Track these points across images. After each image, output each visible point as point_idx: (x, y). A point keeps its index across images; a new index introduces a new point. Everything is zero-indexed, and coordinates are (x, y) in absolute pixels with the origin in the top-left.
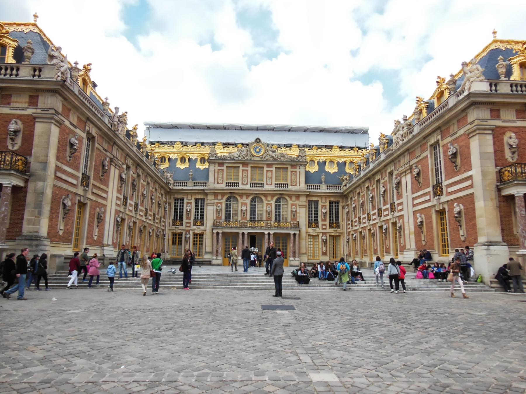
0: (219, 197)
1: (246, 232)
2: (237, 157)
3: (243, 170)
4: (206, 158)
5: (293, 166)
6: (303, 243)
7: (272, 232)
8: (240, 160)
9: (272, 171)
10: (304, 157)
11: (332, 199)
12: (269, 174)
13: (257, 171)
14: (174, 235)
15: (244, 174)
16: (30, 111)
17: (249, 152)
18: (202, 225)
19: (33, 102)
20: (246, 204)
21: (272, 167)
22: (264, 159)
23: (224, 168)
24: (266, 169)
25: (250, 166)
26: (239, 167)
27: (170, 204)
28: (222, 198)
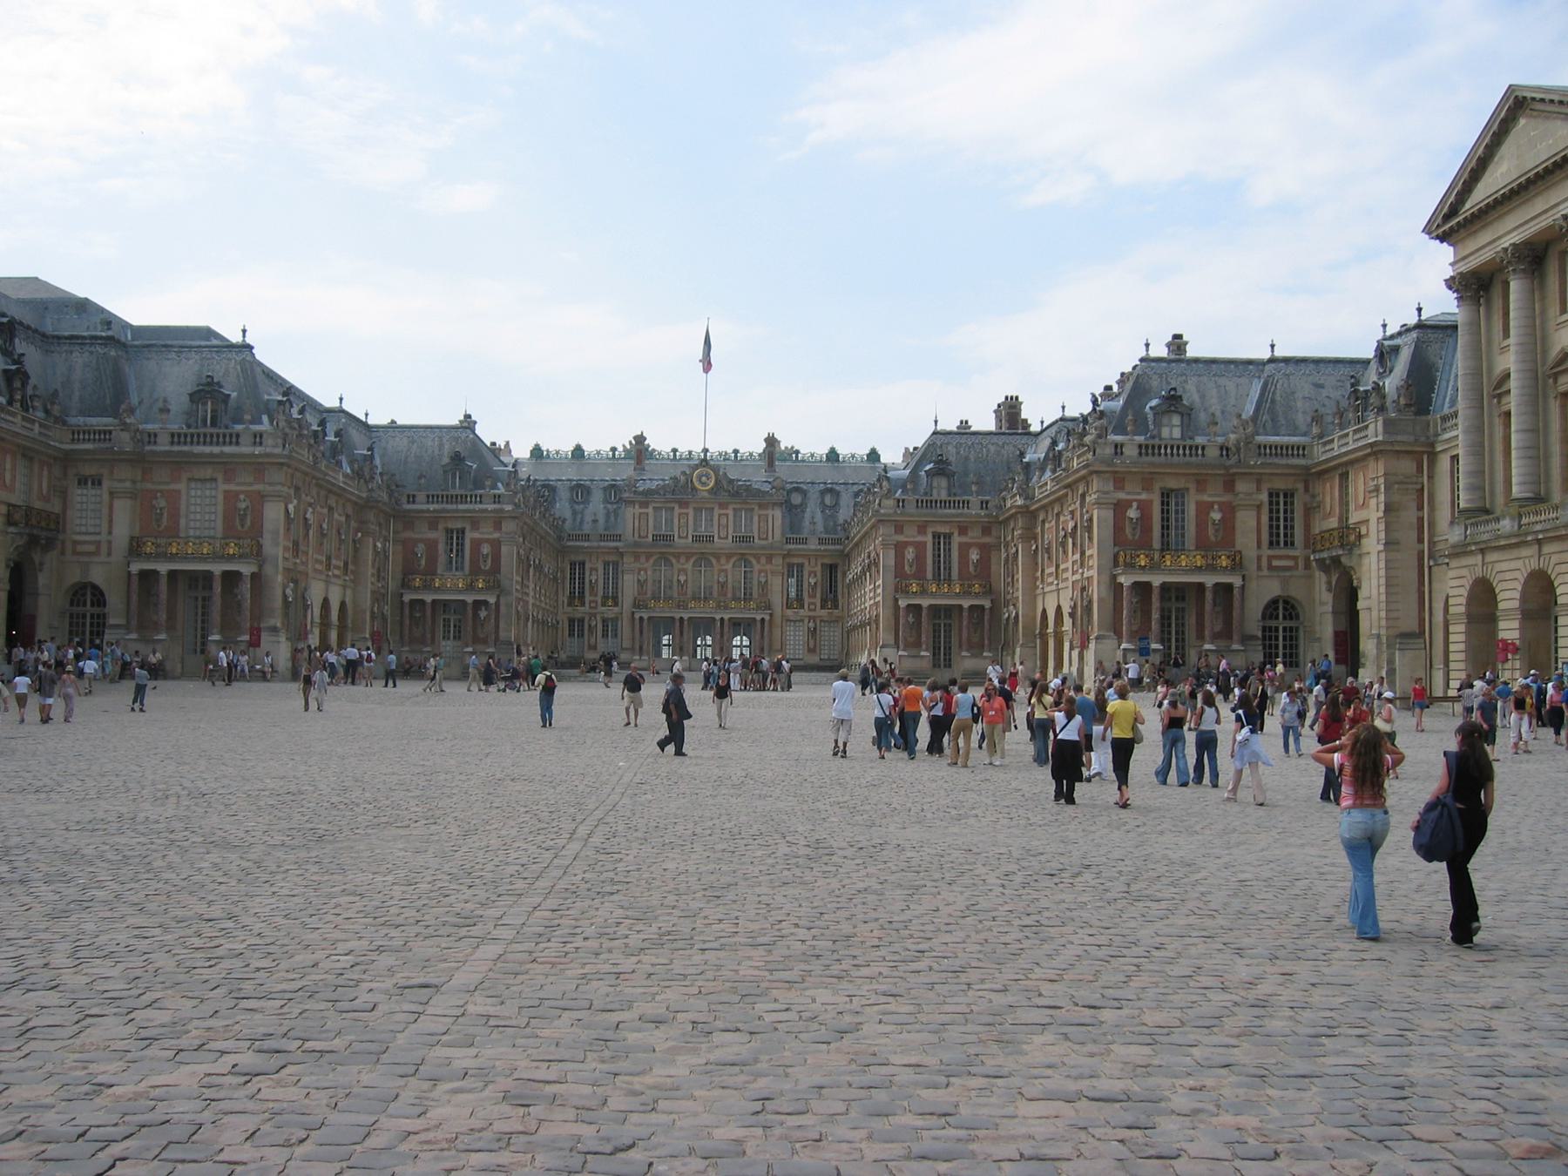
0: (643, 559)
1: (686, 616)
5: (761, 506)
6: (777, 632)
7: (726, 617)
11: (827, 561)
12: (724, 521)
14: (572, 621)
16: (496, 535)
18: (616, 604)
19: (498, 525)
20: (685, 571)
23: (650, 510)
24: (717, 512)
27: (563, 571)
28: (647, 560)
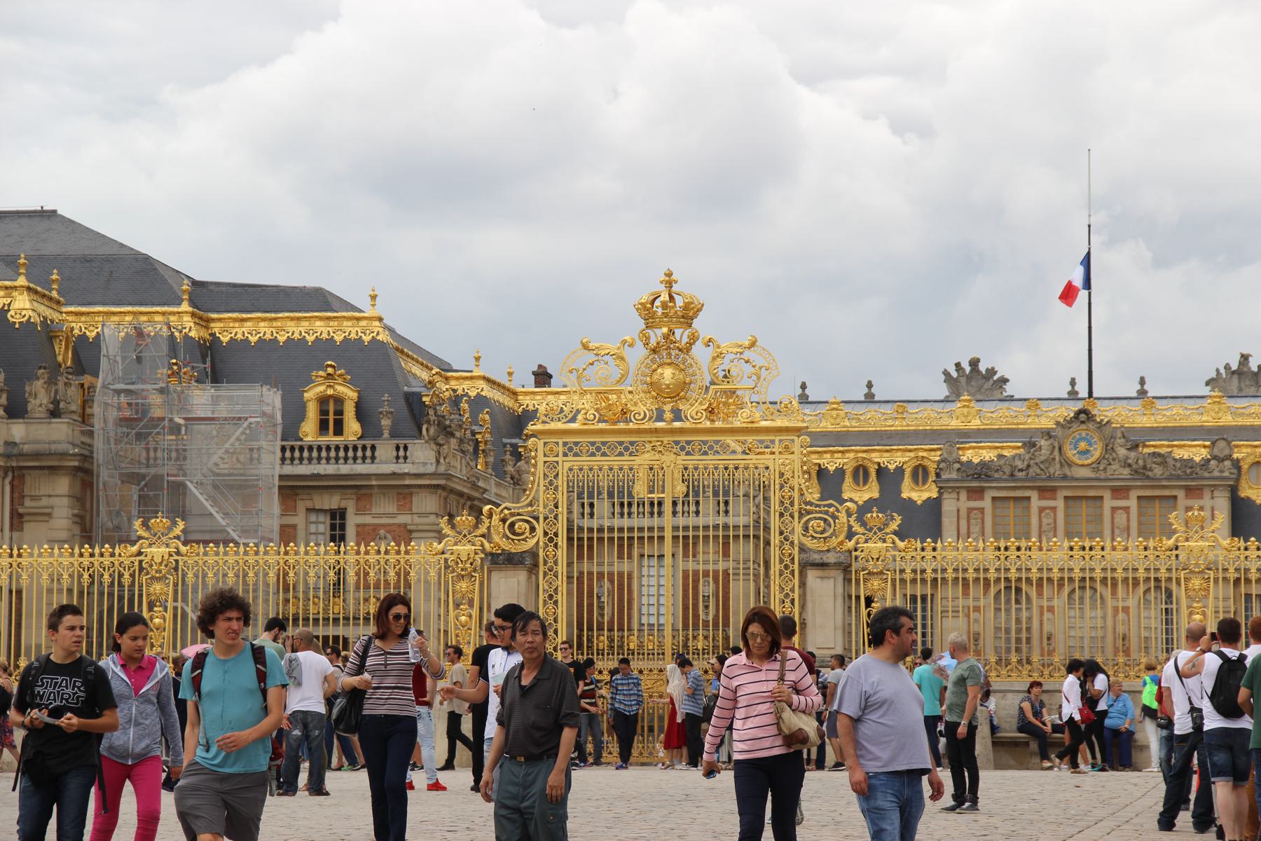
2: (1021, 470)
3: (1042, 510)
4: (932, 468)
8: (1033, 479)
9: (1127, 509)
10: (1227, 463)
12: (1121, 518)
13: (1084, 509)
15: (1045, 521)
17: (1056, 453)
21: (1127, 498)
22: (1103, 475)
23: (986, 503)
24: (1109, 503)
25: (1061, 494)
26: (1029, 498)
